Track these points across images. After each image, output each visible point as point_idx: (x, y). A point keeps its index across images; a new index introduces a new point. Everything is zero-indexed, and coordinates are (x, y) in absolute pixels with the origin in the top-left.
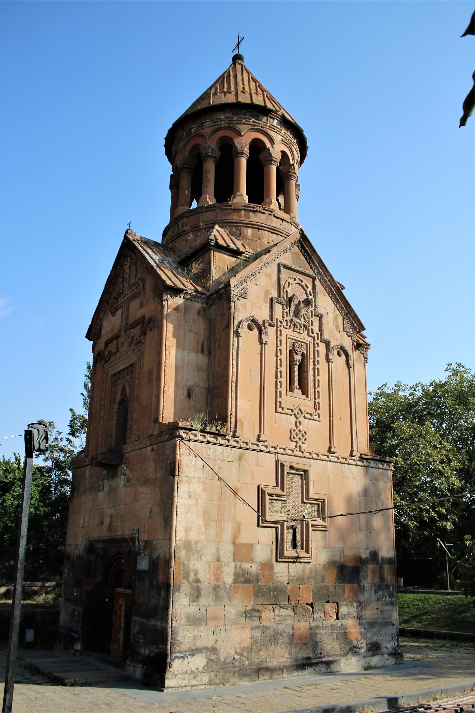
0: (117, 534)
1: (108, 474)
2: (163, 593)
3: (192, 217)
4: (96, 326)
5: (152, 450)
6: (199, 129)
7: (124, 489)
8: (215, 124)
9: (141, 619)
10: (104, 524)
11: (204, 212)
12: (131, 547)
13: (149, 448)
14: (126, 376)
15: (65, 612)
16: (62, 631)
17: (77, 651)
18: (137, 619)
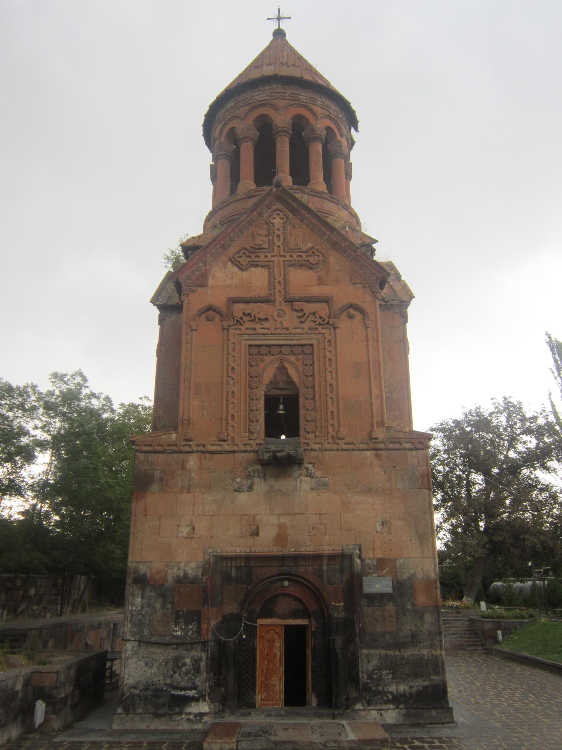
0: (302, 550)
2: (428, 617)
3: (315, 199)
4: (194, 269)
5: (377, 456)
6: (308, 101)
8: (325, 107)
9: (383, 652)
10: (261, 534)
11: (328, 200)
12: (322, 566)
13: (368, 453)
14: (288, 354)
15: (142, 663)
16: (137, 692)
17: (202, 715)
18: (373, 652)
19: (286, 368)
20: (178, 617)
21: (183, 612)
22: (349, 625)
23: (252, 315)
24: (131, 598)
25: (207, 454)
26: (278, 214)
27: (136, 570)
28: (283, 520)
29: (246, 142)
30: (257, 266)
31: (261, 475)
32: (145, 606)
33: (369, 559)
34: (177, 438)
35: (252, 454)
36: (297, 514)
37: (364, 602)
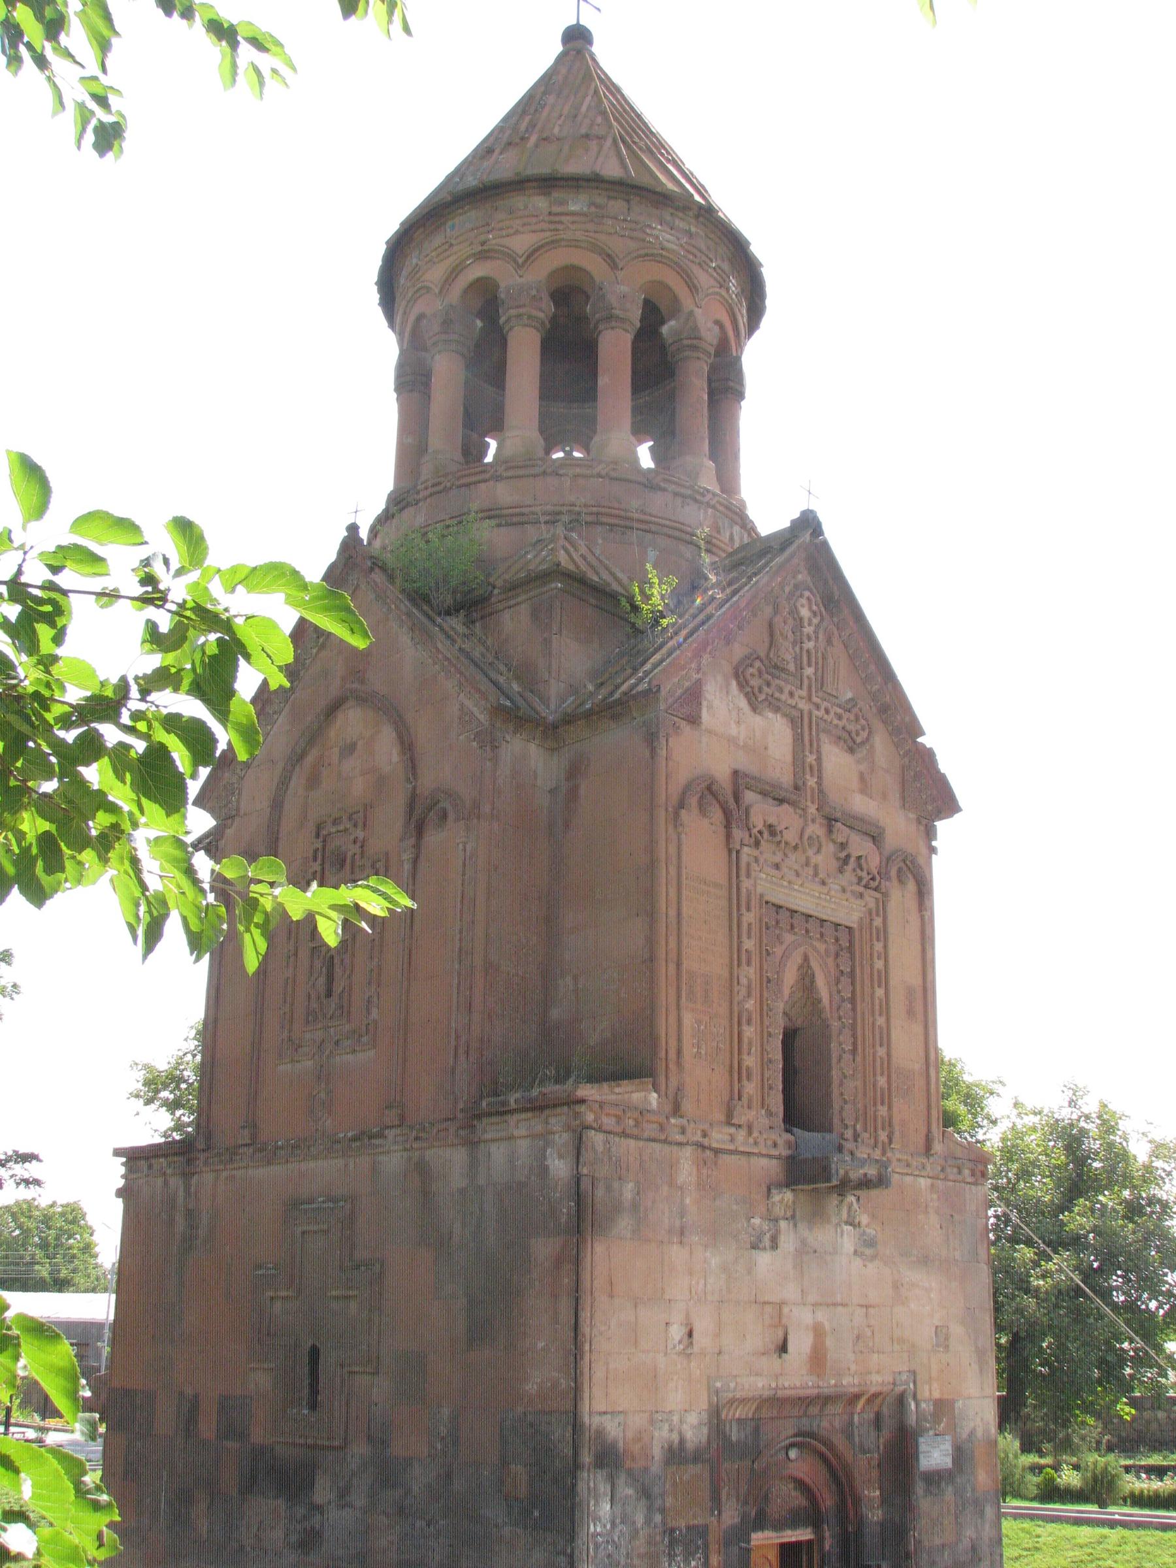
1: (794, 1202)
7: (858, 1262)
10: (791, 1347)
12: (852, 1414)
13: (922, 1181)
19: (809, 967)
20: (672, 1543)
21: (681, 1531)
22: (897, 1533)
23: (778, 829)
24: (592, 1503)
25: (708, 1152)
26: (808, 598)
27: (600, 1433)
28: (821, 1316)
29: (627, 331)
30: (777, 710)
31: (789, 1214)
32: (618, 1521)
33: (925, 1401)
34: (659, 1103)
35: (774, 1161)
36: (835, 1305)
37: (920, 1488)
